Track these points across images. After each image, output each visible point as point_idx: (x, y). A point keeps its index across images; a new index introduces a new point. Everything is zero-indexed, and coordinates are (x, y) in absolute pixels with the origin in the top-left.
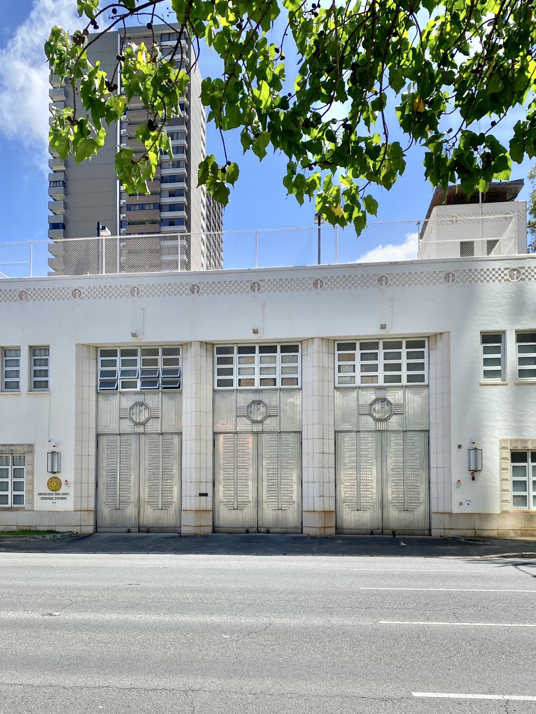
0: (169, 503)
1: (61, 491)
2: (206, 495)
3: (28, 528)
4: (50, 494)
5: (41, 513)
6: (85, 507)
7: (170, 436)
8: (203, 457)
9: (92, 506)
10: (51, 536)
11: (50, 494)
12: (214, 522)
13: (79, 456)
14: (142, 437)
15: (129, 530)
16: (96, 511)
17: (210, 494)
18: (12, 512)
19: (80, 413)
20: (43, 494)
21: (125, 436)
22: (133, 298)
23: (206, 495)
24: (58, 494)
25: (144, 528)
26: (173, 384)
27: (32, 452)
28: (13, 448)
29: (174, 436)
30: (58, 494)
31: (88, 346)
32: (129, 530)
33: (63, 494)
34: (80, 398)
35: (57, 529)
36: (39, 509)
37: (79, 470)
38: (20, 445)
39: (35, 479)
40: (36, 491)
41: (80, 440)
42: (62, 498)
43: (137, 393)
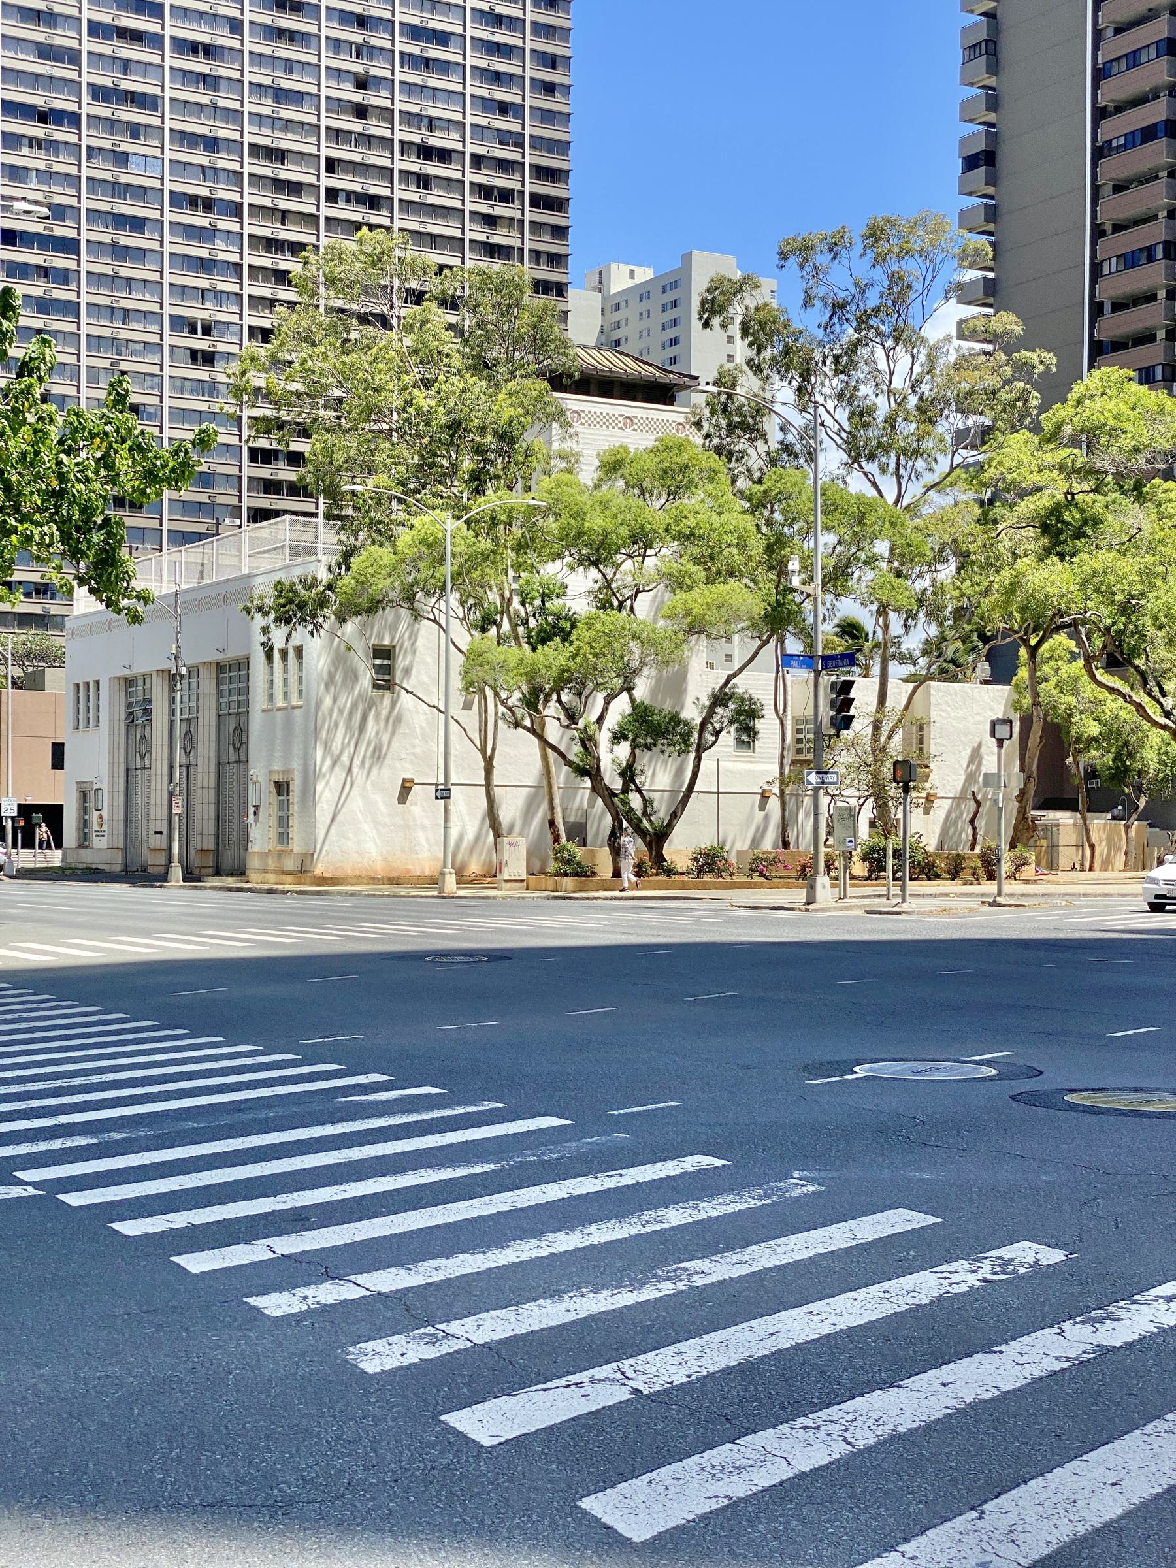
13: (111, 792)
19: (112, 748)
34: (112, 734)
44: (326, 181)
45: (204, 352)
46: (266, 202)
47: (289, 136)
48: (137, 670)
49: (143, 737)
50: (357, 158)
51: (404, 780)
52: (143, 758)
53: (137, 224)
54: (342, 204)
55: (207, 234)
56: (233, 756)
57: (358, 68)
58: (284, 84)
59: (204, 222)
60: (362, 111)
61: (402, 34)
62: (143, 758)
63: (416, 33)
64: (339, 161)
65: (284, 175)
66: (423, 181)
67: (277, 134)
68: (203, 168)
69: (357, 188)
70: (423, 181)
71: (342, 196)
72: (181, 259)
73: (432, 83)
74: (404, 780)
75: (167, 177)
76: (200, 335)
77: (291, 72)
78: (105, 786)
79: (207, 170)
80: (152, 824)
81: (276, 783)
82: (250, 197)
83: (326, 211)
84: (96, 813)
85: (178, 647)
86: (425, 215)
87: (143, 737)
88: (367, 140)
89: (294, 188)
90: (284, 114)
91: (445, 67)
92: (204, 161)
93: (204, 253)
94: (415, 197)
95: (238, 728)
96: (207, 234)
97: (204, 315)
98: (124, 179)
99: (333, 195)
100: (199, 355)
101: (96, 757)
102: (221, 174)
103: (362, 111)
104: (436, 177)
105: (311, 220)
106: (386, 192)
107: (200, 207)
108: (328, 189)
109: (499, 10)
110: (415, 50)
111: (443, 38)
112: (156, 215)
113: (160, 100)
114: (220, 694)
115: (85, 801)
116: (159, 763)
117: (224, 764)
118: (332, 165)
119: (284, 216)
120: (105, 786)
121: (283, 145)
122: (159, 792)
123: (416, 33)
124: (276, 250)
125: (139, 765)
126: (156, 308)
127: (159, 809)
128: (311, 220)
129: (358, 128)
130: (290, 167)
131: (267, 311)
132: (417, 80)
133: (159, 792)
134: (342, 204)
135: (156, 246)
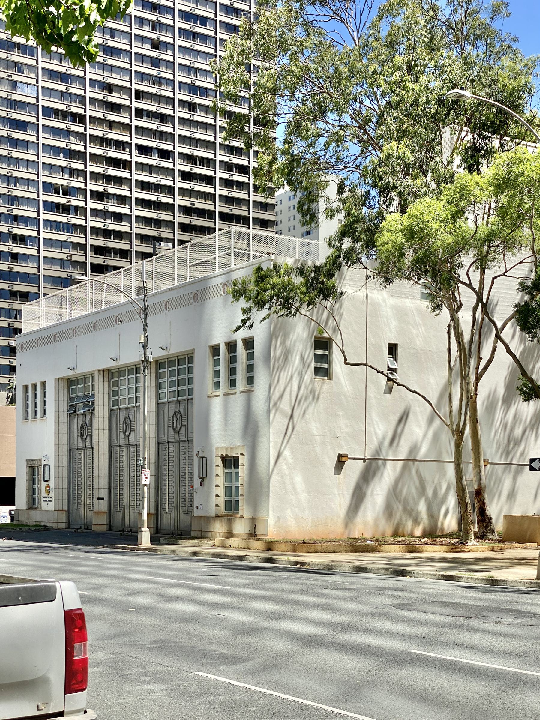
2: (103, 499)
6: (61, 508)
8: (61, 469)
9: (65, 508)
10: (26, 528)
12: (110, 522)
13: (57, 467)
16: (69, 512)
17: (106, 498)
19: (57, 434)
23: (103, 499)
31: (63, 379)
34: (57, 422)
37: (57, 478)
41: (57, 455)
44: (136, 104)
45: (63, 205)
46: (100, 115)
47: (114, 75)
48: (83, 369)
49: (84, 424)
50: (153, 91)
51: (340, 456)
52: (84, 441)
53: (23, 126)
54: (144, 118)
55: (66, 133)
56: (123, 440)
57: (154, 36)
58: (111, 44)
59: (63, 126)
60: (156, 62)
61: (179, 16)
62: (84, 441)
63: (188, 16)
64: (143, 92)
65: (110, 99)
66: (192, 107)
67: (106, 74)
68: (62, 93)
69: (153, 109)
70: (192, 107)
71: (145, 113)
72: (49, 148)
73: (197, 47)
74: (340, 456)
75: (40, 97)
76: (61, 195)
77: (114, 37)
78: (52, 463)
79: (64, 94)
80: (95, 492)
81: (223, 458)
82: (91, 112)
83: (136, 122)
84: (44, 484)
85: (146, 337)
86: (194, 127)
87: (84, 424)
88: (158, 81)
89: (117, 108)
90: (110, 62)
91: (204, 38)
92: (63, 88)
93: (63, 145)
94: (187, 116)
95: (177, 413)
96: (66, 133)
97: (64, 182)
98: (15, 97)
99: (139, 113)
100: (61, 207)
101: (45, 438)
102: (73, 98)
103: (156, 62)
104: (200, 105)
105: (127, 127)
106: (170, 112)
107: (61, 117)
108: (136, 109)
109: (236, 5)
110: (187, 27)
111: (203, 21)
112: (34, 120)
113: (35, 50)
114: (159, 386)
115: (33, 474)
116: (101, 444)
117: (164, 443)
118: (139, 95)
119: (111, 124)
120: (52, 463)
121: (110, 81)
122: (101, 467)
123: (188, 16)
124: (106, 144)
125: (80, 445)
126: (34, 177)
127: (101, 480)
128: (127, 127)
129: (154, 73)
130: (114, 94)
131: (101, 182)
132: (188, 45)
133: (101, 467)
134: (144, 118)
135: (34, 139)
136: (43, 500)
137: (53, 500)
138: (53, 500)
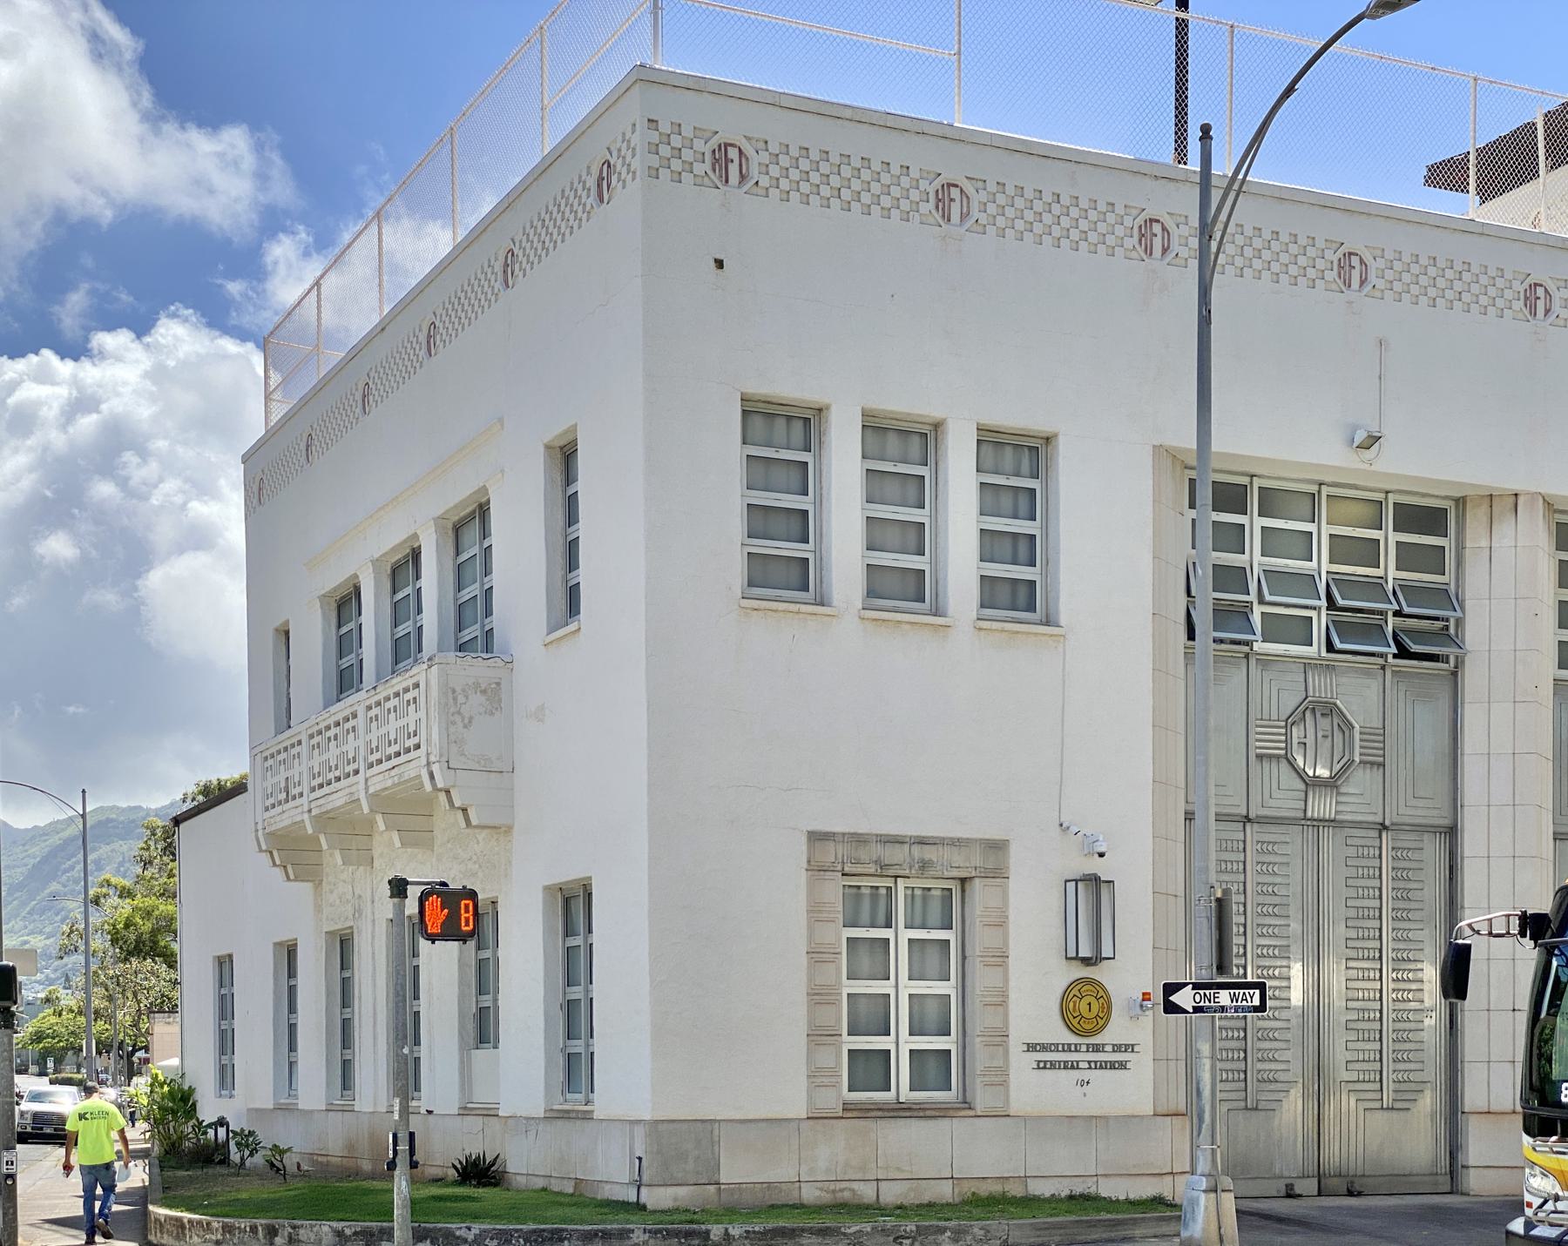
0: (1413, 1086)
1: (1112, 1034)
3: (996, 1188)
4: (1068, 1048)
5: (1036, 1123)
7: (1412, 836)
11: (1068, 1048)
14: (1327, 834)
15: (1290, 1187)
18: (932, 1123)
20: (1045, 1048)
21: (1273, 828)
22: (1349, 295)
24: (1097, 1048)
25: (1336, 1181)
26: (1422, 641)
27: (998, 874)
28: (930, 853)
29: (1426, 836)
30: (1097, 1048)
32: (1290, 1187)
33: (1117, 1048)
35: (1109, 1189)
36: (1029, 1110)
38: (956, 843)
39: (1012, 984)
40: (1019, 1033)
42: (1112, 1066)
43: (1307, 665)
136: (1021, 1064)
137: (1142, 1065)
138: (1142, 1065)
